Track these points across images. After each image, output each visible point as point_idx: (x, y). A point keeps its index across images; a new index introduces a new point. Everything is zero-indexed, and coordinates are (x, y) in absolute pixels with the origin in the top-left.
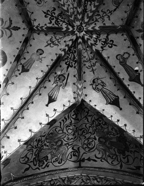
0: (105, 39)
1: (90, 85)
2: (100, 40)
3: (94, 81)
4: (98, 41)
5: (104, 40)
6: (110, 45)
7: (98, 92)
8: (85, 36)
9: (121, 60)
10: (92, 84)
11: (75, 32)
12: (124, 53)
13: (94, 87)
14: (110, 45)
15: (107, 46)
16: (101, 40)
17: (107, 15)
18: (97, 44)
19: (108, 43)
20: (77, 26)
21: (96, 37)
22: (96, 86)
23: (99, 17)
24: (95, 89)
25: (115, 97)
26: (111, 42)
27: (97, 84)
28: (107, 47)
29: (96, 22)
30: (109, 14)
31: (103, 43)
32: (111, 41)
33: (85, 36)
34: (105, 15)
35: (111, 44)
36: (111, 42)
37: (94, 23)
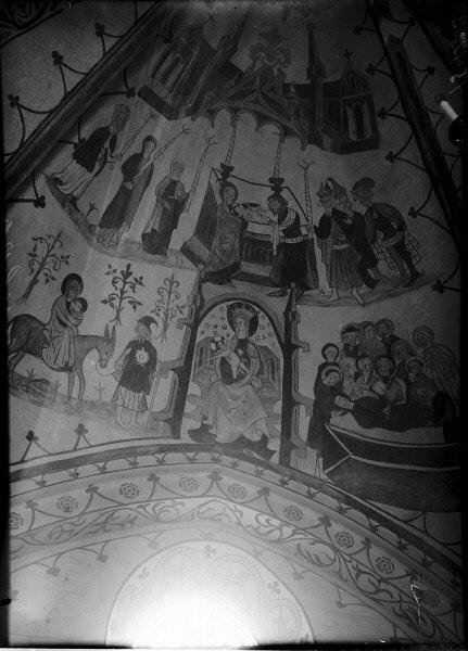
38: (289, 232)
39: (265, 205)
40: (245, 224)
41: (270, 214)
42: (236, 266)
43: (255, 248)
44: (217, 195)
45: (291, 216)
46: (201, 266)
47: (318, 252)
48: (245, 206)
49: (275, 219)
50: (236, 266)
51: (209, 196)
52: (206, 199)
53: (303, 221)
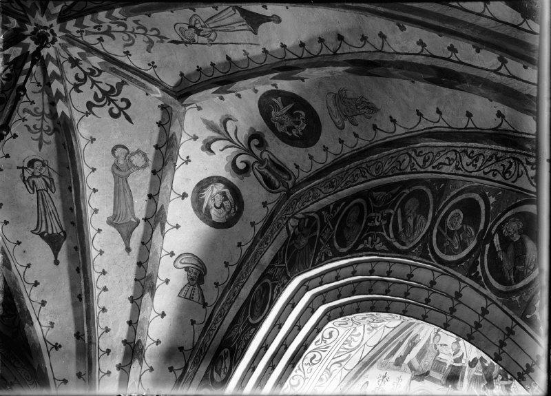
0: (112, 87)
1: (18, 167)
2: (94, 82)
3: (31, 164)
4: (89, 82)
5: (108, 89)
6: (116, 111)
7: (31, 191)
8: (50, 63)
9: (121, 162)
10: (23, 168)
11: (25, 37)
12: (138, 152)
13: (27, 174)
14: (116, 111)
15: (107, 108)
16: (99, 85)
17: (149, 38)
18: (80, 88)
19: (113, 101)
20: (36, 25)
21: (89, 71)
22: (33, 175)
23: (122, 28)
24: (28, 180)
25: (59, 231)
26: (123, 105)
27: (37, 174)
28: (102, 112)
29: (105, 37)
30: (155, 39)
31: (100, 96)
32: (123, 100)
33: (50, 63)
34: (144, 34)
35: (121, 109)
36: (123, 105)
37: (99, 36)
38: (456, 361)
39: (450, 346)
40: (438, 354)
41: (451, 350)
42: (427, 373)
43: (438, 365)
44: (432, 340)
45: (460, 354)
46: (413, 372)
47: (466, 373)
48: (441, 345)
49: (452, 353)
50: (427, 373)
51: (428, 341)
52: (427, 342)
53: (465, 357)
